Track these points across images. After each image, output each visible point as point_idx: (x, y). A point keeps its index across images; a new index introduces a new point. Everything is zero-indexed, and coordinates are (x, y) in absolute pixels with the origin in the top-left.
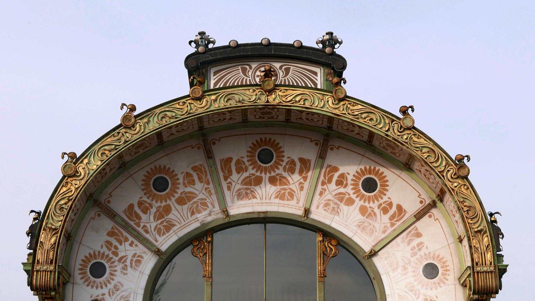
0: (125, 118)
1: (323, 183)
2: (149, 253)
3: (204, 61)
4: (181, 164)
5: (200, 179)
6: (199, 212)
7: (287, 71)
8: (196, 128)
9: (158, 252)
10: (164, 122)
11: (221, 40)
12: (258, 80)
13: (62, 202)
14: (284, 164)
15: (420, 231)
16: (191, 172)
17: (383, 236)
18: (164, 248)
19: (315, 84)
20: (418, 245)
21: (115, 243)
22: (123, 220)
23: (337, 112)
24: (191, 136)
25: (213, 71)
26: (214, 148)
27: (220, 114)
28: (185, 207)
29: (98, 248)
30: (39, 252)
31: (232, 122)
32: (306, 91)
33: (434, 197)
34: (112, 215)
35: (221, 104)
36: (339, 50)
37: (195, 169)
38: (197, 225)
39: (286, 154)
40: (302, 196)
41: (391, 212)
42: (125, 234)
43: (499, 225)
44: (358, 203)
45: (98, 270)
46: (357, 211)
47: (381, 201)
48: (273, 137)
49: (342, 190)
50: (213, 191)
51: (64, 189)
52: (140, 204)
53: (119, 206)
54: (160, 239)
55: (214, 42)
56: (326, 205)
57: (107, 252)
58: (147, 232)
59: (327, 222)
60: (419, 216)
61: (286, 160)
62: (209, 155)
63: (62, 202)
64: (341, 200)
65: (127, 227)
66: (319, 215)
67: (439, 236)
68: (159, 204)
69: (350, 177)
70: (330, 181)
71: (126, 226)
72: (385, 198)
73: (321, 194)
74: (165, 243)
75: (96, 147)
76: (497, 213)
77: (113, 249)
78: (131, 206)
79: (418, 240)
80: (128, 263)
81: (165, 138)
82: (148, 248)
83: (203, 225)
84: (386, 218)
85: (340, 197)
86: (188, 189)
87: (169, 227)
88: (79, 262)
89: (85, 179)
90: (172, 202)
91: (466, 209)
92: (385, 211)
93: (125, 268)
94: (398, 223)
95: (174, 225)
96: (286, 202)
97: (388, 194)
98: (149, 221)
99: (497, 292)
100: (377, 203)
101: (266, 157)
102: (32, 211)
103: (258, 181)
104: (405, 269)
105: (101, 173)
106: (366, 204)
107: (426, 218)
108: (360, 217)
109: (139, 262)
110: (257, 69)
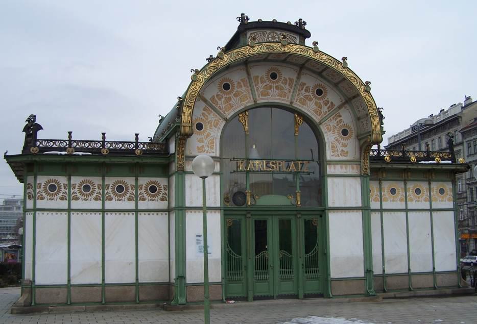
1: (299, 91)
3: (246, 27)
4: (236, 77)
6: (244, 101)
9: (226, 120)
11: (253, 19)
13: (193, 93)
14: (282, 80)
15: (341, 114)
21: (206, 114)
25: (250, 33)
27: (259, 55)
28: (238, 98)
30: (183, 117)
33: (347, 99)
36: (306, 27)
37: (242, 80)
38: (243, 107)
43: (382, 113)
47: (324, 100)
49: (307, 94)
50: (250, 91)
53: (208, 96)
58: (220, 109)
59: (300, 108)
60: (340, 107)
62: (249, 75)
63: (193, 93)
64: (307, 98)
66: (297, 105)
67: (346, 117)
69: (311, 88)
70: (302, 90)
71: (210, 106)
72: (326, 99)
74: (229, 114)
76: (382, 108)
77: (206, 117)
79: (339, 119)
80: (213, 124)
82: (221, 117)
83: (245, 107)
84: (326, 108)
85: (306, 97)
86: (239, 90)
87: (231, 106)
89: (203, 82)
90: (232, 95)
92: (326, 105)
93: (211, 126)
96: (283, 98)
98: (221, 103)
100: (322, 101)
104: (334, 131)
107: (343, 109)
108: (315, 107)
109: (217, 124)
110: (269, 34)
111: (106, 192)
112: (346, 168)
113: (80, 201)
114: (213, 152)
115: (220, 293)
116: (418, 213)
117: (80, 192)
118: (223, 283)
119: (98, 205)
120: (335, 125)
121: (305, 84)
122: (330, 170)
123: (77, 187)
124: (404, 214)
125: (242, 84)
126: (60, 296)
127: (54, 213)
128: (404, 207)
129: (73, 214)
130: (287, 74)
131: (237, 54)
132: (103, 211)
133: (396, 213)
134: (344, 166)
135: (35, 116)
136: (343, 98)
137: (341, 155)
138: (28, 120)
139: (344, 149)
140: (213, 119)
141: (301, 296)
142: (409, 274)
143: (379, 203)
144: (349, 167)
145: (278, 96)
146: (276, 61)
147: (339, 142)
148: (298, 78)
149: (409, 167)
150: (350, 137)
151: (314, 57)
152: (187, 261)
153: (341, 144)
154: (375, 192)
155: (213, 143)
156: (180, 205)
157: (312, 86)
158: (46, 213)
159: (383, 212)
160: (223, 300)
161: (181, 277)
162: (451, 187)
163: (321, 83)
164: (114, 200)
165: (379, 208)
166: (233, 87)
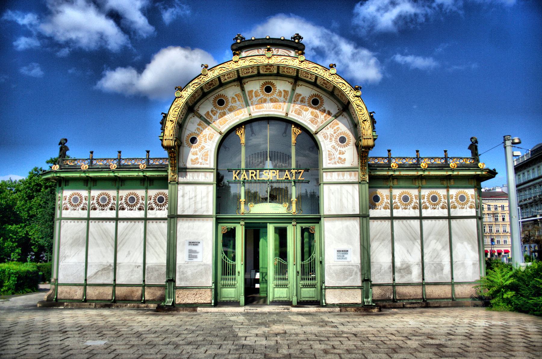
0: (204, 71)
2: (216, 133)
10: (221, 72)
22: (205, 119)
24: (234, 81)
26: (245, 86)
29: (194, 131)
37: (236, 95)
38: (238, 120)
39: (277, 88)
43: (374, 117)
45: (193, 140)
46: (310, 114)
48: (272, 81)
52: (212, 111)
53: (203, 112)
59: (296, 119)
61: (277, 91)
62: (243, 89)
66: (292, 116)
68: (220, 111)
69: (306, 99)
70: (297, 101)
75: (190, 84)
78: (208, 113)
80: (207, 137)
83: (240, 120)
88: (185, 137)
90: (226, 110)
93: (206, 139)
97: (324, 106)
102: (162, 113)
103: (265, 101)
104: (331, 139)
105: (193, 96)
108: (311, 116)
112: (343, 175)
113: (97, 211)
114: (207, 164)
116: (433, 221)
118: (213, 287)
121: (300, 95)
122: (326, 177)
124: (417, 222)
125: (237, 99)
126: (77, 293)
128: (418, 215)
130: (282, 86)
132: (117, 219)
134: (341, 173)
136: (340, 107)
138: (60, 143)
139: (341, 156)
140: (208, 133)
143: (389, 211)
145: (273, 108)
146: (270, 75)
148: (293, 90)
150: (348, 144)
152: (177, 266)
153: (338, 151)
154: (385, 200)
155: (206, 155)
156: (173, 213)
157: (308, 96)
159: (394, 220)
160: (211, 303)
162: (474, 194)
164: (126, 209)
165: (389, 216)
166: (227, 102)
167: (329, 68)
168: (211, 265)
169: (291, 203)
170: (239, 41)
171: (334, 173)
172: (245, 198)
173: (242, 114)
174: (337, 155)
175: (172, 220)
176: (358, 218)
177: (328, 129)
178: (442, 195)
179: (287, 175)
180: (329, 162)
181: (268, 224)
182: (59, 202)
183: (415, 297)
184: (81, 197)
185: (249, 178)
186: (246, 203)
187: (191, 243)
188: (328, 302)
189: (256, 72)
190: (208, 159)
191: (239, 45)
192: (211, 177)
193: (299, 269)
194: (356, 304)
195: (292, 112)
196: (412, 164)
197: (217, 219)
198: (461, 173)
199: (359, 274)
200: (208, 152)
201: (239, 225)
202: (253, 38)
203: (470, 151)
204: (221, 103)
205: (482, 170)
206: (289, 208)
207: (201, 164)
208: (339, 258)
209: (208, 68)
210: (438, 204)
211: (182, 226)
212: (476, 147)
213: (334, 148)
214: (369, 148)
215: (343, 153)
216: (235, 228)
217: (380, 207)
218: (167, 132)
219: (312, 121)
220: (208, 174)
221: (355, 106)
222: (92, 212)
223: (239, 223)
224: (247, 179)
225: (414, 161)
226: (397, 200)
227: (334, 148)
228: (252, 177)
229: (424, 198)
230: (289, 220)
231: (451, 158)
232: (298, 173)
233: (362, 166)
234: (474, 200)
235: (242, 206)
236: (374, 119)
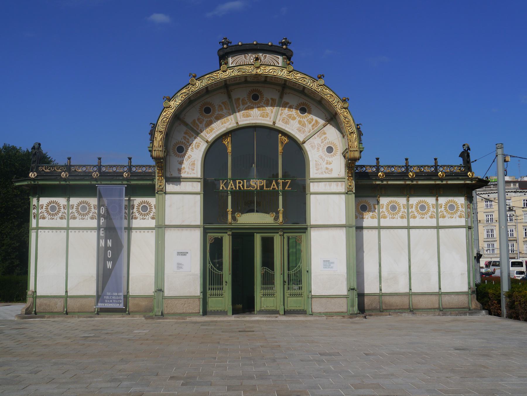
4: (217, 100)
5: (226, 108)
6: (225, 123)
7: (265, 56)
8: (223, 84)
9: (207, 142)
12: (252, 61)
16: (221, 104)
17: (309, 134)
18: (209, 140)
19: (278, 63)
20: (325, 138)
21: (187, 137)
22: (191, 127)
23: (289, 77)
24: (221, 88)
27: (235, 78)
31: (240, 81)
32: (275, 68)
34: (186, 124)
35: (236, 73)
38: (224, 129)
40: (273, 115)
41: (313, 123)
42: (192, 133)
43: (361, 129)
44: (298, 119)
46: (297, 123)
47: (308, 118)
49: (290, 113)
51: (165, 114)
52: (198, 119)
53: (189, 120)
54: (208, 135)
55: (231, 43)
56: (283, 120)
57: (184, 141)
61: (265, 99)
62: (230, 97)
65: (192, 130)
66: (280, 125)
73: (281, 115)
78: (194, 121)
79: (324, 136)
80: (194, 146)
81: (209, 89)
84: (310, 126)
89: (175, 108)
90: (213, 118)
91: (346, 122)
92: (310, 123)
94: (316, 128)
95: (214, 129)
99: (359, 160)
101: (255, 98)
104: (318, 149)
106: (301, 119)
108: (299, 125)
109: (198, 146)
111: (71, 211)
112: (330, 185)
115: (198, 307)
116: (421, 230)
117: (78, 212)
118: (202, 297)
119: (63, 223)
120: (320, 143)
122: (313, 187)
123: (75, 207)
125: (223, 107)
126: (57, 306)
127: (54, 231)
128: (406, 225)
129: (71, 232)
131: (208, 79)
133: (396, 230)
134: (328, 183)
135: (40, 144)
137: (325, 172)
139: (328, 166)
141: (282, 312)
142: (410, 294)
143: (376, 220)
144: (334, 184)
147: (323, 160)
149: (408, 182)
151: (288, 77)
153: (325, 161)
155: (193, 164)
158: (47, 231)
161: (160, 290)
163: (305, 101)
165: (377, 225)
167: (317, 78)
168: (199, 275)
169: (277, 213)
170: (225, 46)
171: (320, 183)
172: (232, 208)
173: (229, 123)
174: (324, 165)
175: (160, 229)
176: (344, 228)
177: (315, 138)
178: (431, 205)
179: (274, 186)
180: (317, 172)
181: (255, 234)
182: (35, 211)
183: (402, 307)
184: (59, 205)
185: (236, 187)
186: (233, 213)
187: (179, 254)
188: (314, 311)
189: (243, 80)
190: (195, 169)
191: (226, 51)
192: (198, 187)
193: (286, 279)
194: (342, 312)
195: (279, 121)
196: (400, 173)
197: (205, 229)
198: (449, 182)
199: (345, 283)
200: (194, 161)
201: (226, 235)
202: (240, 44)
203: (461, 159)
204: (208, 110)
205: (471, 179)
206: (276, 218)
207: (188, 173)
208: (325, 267)
209: (196, 78)
210: (426, 213)
211: (170, 235)
212: (468, 156)
213: (321, 157)
214: (355, 160)
215: (330, 163)
216: (222, 238)
217: (367, 217)
218: (156, 144)
219: (300, 131)
220: (195, 184)
221: (342, 118)
222: (71, 221)
223: (226, 233)
224: (234, 189)
225: (403, 169)
226: (384, 209)
227: (321, 157)
228: (239, 186)
229: (412, 207)
230: (275, 230)
231: (441, 166)
232: (284, 184)
233: (348, 176)
234: (464, 210)
235: (230, 217)
236: (361, 132)
